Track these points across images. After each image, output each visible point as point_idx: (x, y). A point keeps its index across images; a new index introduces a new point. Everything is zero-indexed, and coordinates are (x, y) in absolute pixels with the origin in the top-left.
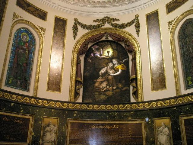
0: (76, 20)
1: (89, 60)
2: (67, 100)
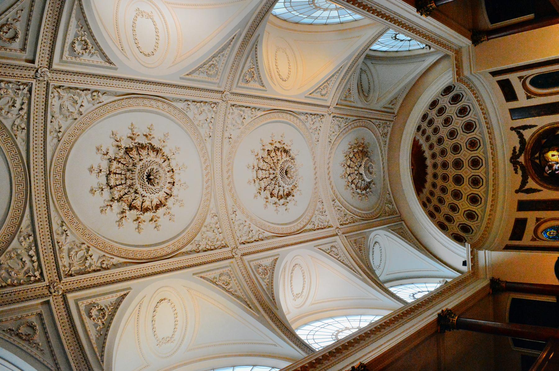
0: (517, 192)
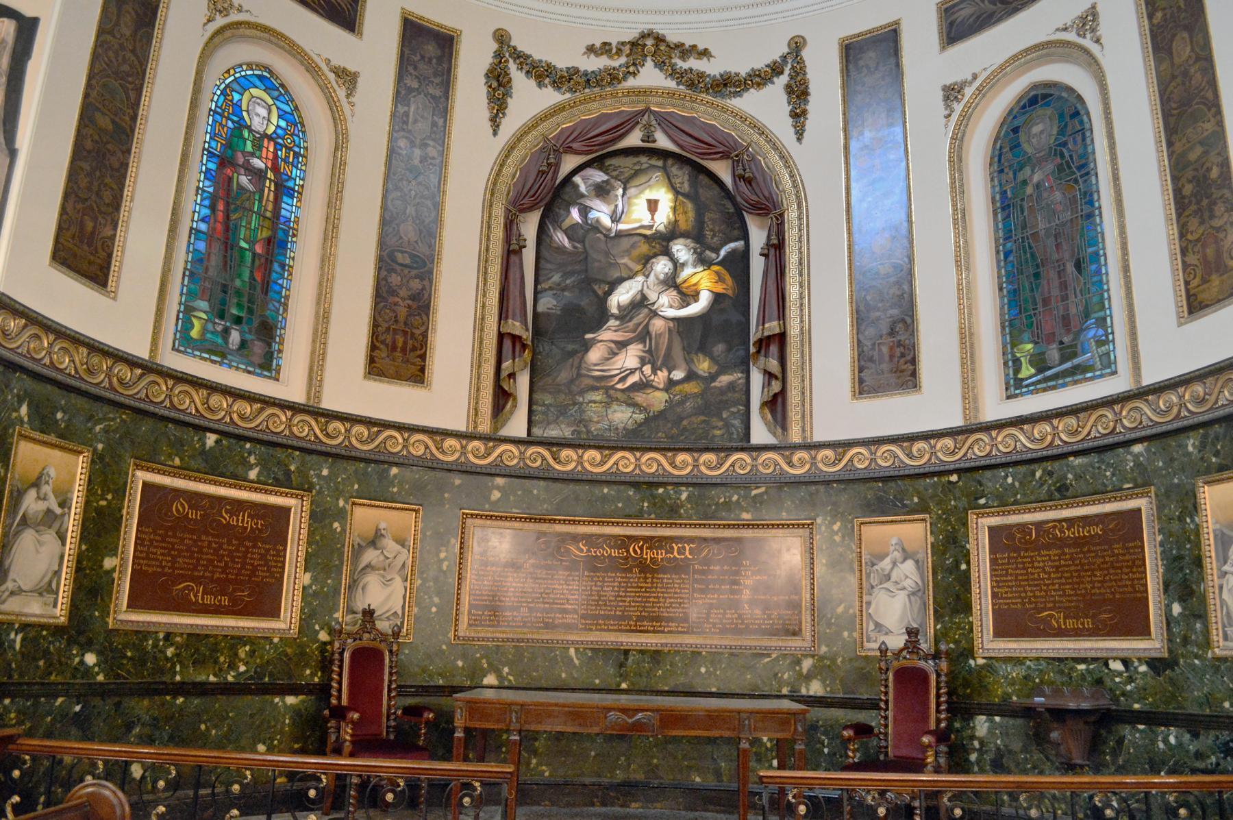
0: (501, 37)
1: (561, 238)
2: (462, 427)
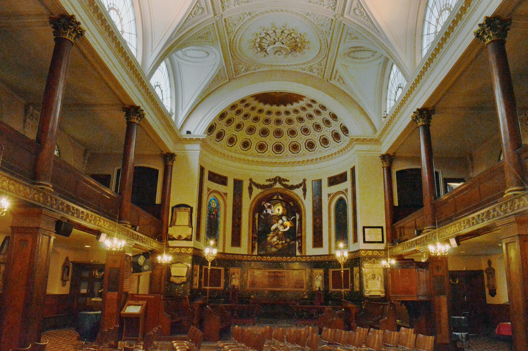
0: (251, 180)
1: (262, 216)
2: (247, 253)
